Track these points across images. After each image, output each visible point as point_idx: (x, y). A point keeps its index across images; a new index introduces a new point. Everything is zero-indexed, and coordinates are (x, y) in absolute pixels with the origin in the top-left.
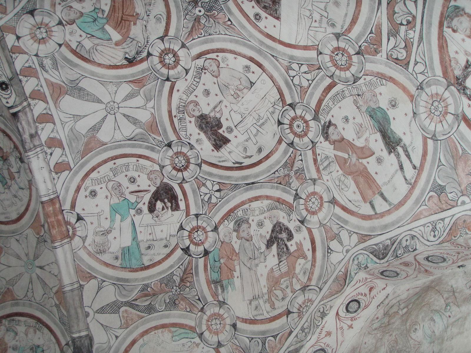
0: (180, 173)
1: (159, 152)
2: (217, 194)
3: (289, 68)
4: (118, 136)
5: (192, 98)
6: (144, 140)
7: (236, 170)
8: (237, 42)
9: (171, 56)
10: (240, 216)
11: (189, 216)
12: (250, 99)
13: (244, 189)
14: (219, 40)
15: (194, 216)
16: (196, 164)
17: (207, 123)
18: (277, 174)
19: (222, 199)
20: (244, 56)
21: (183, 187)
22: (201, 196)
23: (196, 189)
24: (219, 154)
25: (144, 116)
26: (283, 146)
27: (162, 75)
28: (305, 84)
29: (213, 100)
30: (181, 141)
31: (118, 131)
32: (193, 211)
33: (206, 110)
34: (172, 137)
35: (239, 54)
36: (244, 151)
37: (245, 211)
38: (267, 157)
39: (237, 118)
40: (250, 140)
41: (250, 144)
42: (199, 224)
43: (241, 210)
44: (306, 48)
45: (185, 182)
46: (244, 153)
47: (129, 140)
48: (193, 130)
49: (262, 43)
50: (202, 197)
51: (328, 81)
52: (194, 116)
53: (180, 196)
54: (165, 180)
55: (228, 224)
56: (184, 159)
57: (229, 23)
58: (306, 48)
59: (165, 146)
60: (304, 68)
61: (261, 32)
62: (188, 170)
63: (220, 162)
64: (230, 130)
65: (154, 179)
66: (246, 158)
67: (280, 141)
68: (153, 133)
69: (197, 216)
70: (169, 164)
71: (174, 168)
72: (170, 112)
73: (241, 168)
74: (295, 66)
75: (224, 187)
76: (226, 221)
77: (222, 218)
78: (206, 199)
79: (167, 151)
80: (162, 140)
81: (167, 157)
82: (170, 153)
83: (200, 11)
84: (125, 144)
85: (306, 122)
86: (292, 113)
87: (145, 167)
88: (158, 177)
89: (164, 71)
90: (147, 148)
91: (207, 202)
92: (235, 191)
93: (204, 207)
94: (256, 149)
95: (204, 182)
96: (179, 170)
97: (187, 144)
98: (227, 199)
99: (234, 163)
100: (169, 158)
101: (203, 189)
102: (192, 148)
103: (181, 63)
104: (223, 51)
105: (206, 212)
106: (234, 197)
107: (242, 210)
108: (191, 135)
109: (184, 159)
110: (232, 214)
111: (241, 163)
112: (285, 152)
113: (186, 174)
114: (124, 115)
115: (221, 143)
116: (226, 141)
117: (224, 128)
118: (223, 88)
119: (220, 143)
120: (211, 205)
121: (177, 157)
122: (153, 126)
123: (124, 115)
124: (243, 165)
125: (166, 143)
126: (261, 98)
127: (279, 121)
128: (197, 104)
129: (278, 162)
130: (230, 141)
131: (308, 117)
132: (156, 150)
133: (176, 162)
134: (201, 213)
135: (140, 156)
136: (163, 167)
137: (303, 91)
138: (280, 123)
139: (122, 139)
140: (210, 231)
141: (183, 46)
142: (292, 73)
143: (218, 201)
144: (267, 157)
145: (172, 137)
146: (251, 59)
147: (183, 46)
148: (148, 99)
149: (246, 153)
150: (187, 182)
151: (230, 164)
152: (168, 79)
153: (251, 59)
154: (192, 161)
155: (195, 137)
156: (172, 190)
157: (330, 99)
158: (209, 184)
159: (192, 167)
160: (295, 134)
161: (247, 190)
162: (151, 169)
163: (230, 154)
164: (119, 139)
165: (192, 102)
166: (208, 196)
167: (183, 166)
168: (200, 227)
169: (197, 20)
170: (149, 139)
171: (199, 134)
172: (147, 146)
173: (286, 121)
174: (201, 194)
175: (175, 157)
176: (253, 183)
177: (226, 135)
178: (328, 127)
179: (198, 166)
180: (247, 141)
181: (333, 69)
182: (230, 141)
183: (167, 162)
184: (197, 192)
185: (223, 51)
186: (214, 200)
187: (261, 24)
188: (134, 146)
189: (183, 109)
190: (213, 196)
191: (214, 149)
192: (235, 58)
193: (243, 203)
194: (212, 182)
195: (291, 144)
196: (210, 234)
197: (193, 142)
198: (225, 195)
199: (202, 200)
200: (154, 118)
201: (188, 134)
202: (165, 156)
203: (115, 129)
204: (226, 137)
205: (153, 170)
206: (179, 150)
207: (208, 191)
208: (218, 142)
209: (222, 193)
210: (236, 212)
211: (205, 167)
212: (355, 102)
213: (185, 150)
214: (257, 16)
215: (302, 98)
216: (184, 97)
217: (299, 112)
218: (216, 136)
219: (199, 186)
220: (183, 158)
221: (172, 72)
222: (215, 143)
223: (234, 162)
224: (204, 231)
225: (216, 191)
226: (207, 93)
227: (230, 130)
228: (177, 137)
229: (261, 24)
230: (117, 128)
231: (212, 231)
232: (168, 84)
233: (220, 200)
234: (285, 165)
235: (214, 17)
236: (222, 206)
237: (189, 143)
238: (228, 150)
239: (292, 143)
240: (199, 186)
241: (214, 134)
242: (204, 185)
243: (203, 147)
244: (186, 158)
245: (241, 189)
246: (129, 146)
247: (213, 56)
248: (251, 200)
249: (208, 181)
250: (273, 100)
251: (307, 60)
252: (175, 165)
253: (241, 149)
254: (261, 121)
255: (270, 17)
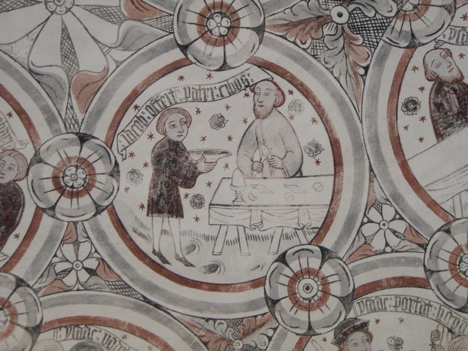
0: (56, 195)
1: (57, 133)
2: (84, 276)
3: (375, 204)
4: (20, 51)
5: (190, 108)
6: (53, 95)
7: (148, 265)
8: (341, 104)
9: (226, 22)
10: (95, 340)
11: (7, 272)
12: (275, 190)
13: (135, 303)
14: (317, 75)
15: (13, 279)
16: (95, 203)
17: (174, 161)
18: (210, 326)
19: (86, 289)
20: (329, 131)
21: (40, 220)
22: (55, 256)
23: (58, 240)
24: (146, 220)
25: (90, 60)
26: (258, 293)
27: (183, 34)
28: (378, 244)
29: (216, 140)
30: (108, 149)
31: (27, 42)
32: (20, 270)
33: (191, 143)
34: (101, 131)
35: (326, 123)
36: (187, 248)
37: (109, 340)
38: (215, 287)
39: (226, 195)
40: (213, 242)
41: (206, 247)
42: (14, 299)
43: (103, 332)
44: (433, 205)
45: (51, 213)
46: (185, 252)
47: (31, 71)
48: (141, 151)
49: (375, 140)
50: (55, 260)
51: (419, 273)
52: (165, 133)
53: (22, 229)
54: (23, 185)
55: (64, 337)
56: (84, 179)
57: (362, 71)
58: (433, 205)
59: (76, 134)
60: (400, 226)
61: (392, 127)
62: (75, 200)
63: (135, 231)
64: (198, 202)
65: (6, 167)
66: (180, 260)
67: (257, 283)
68: (77, 98)
69: (20, 283)
70: (55, 165)
71: (55, 179)
72: (135, 94)
73: (159, 267)
74: (389, 212)
75: (103, 273)
76: (64, 330)
77: (60, 321)
78: (59, 268)
79: (71, 142)
80: (80, 121)
81: (61, 152)
82: (73, 151)
83: (340, 15)
84: (17, 71)
85: (326, 293)
86: (315, 263)
87: (12, 135)
88: (16, 169)
89: (193, 32)
90: (45, 110)
91: (57, 275)
92: (117, 293)
93: (44, 279)
94: (210, 260)
95: (81, 239)
96: (60, 188)
97: (113, 162)
98: (92, 296)
99: (154, 252)
100: (64, 156)
101: (68, 250)
102: (115, 175)
103: (229, 46)
104: (306, 93)
105: (40, 288)
106: (109, 302)
107: (106, 335)
108: (132, 155)
109: (84, 179)
110: (83, 326)
111: (166, 262)
112: (253, 305)
113: (65, 203)
114: (64, 30)
115: (166, 207)
116: (176, 211)
117: (191, 192)
118: (250, 139)
119: (166, 204)
120: (57, 284)
121: (77, 167)
122: (88, 89)
123: (64, 30)
124: (166, 266)
125: (81, 131)
126: (291, 204)
127: (284, 254)
128: (187, 122)
129: (227, 308)
130: (182, 216)
131: (336, 289)
132: (56, 127)
133: (68, 173)
134: (31, 283)
135: (21, 113)
136: (40, 161)
137: (365, 250)
138: (282, 259)
139: (21, 60)
140: (22, 327)
141: (260, 30)
142: (373, 214)
143: (76, 288)
144: (215, 287)
145: (101, 131)
146: (335, 144)
147: (260, 30)
148: (123, 44)
149: (188, 253)
150: (53, 216)
151: (146, 248)
152: (184, 48)
153: (335, 144)
154: (95, 193)
155: (135, 163)
156: (18, 210)
157: (396, 296)
158: (85, 249)
159: (85, 201)
160: (292, 294)
161: (138, 308)
162: (18, 146)
163: (163, 235)
164: (18, 55)
165: (183, 112)
166: (67, 266)
167: (72, 187)
168: (10, 306)
169: (322, 20)
170: (62, 99)
171: (146, 165)
172: (48, 107)
173: (295, 266)
174: (59, 254)
175: (74, 162)
176: (157, 306)
177: (186, 203)
178: (357, 329)
179: (97, 208)
180: (207, 238)
181: (443, 265)
182: (182, 216)
183: (54, 160)
184: (54, 245)
185: (306, 93)
186: (70, 280)
187: (403, 119)
188: (27, 88)
189: (160, 109)
190: (73, 272)
191: (146, 206)
192: (314, 121)
193: (115, 324)
194: (93, 251)
195: (272, 303)
196: (19, 333)
197: (124, 167)
198: (96, 286)
199: (51, 264)
200: (104, 78)
201: (129, 150)
202: (57, 149)
203: (28, 35)
204: (181, 206)
205: (21, 151)
206: (91, 160)
207: (72, 258)
208: (162, 202)
209: (94, 280)
210: (92, 328)
211: (104, 218)
212: (436, 335)
213: (100, 167)
214: (412, 105)
215: (352, 257)
216: (180, 95)
217: (327, 270)
218: (168, 191)
219: (66, 238)
220: (84, 176)
221: (200, 45)
222: (155, 199)
223: (157, 250)
224: (12, 318)
225: (88, 270)
226: (219, 122)
227: (198, 202)
228: (107, 138)
229: (403, 119)
230: (33, 36)
231: (26, 329)
232: (177, 55)
233: (81, 288)
234: (235, 323)
235: (349, 42)
236: (76, 301)
237: (117, 164)
238: (166, 227)
239: (275, 302)
240: (66, 238)
241: (169, 185)
242: (77, 243)
243: (134, 189)
244: (90, 179)
245: (131, 299)
246: (21, 80)
247: (285, 86)
248: (133, 330)
249: (88, 244)
250: (304, 221)
251: (417, 220)
252: (61, 175)
253: (186, 241)
254: (256, 232)
255: (428, 122)
